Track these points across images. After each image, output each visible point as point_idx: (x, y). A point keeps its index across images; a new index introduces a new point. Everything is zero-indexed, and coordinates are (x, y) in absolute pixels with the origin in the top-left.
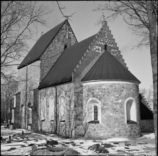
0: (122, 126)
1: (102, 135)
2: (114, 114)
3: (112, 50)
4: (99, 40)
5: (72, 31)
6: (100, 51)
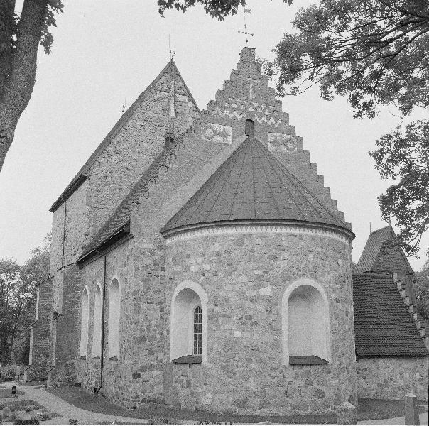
0: (273, 374)
1: (208, 402)
2: (247, 334)
3: (271, 137)
4: (226, 104)
5: (190, 95)
6: (230, 139)
